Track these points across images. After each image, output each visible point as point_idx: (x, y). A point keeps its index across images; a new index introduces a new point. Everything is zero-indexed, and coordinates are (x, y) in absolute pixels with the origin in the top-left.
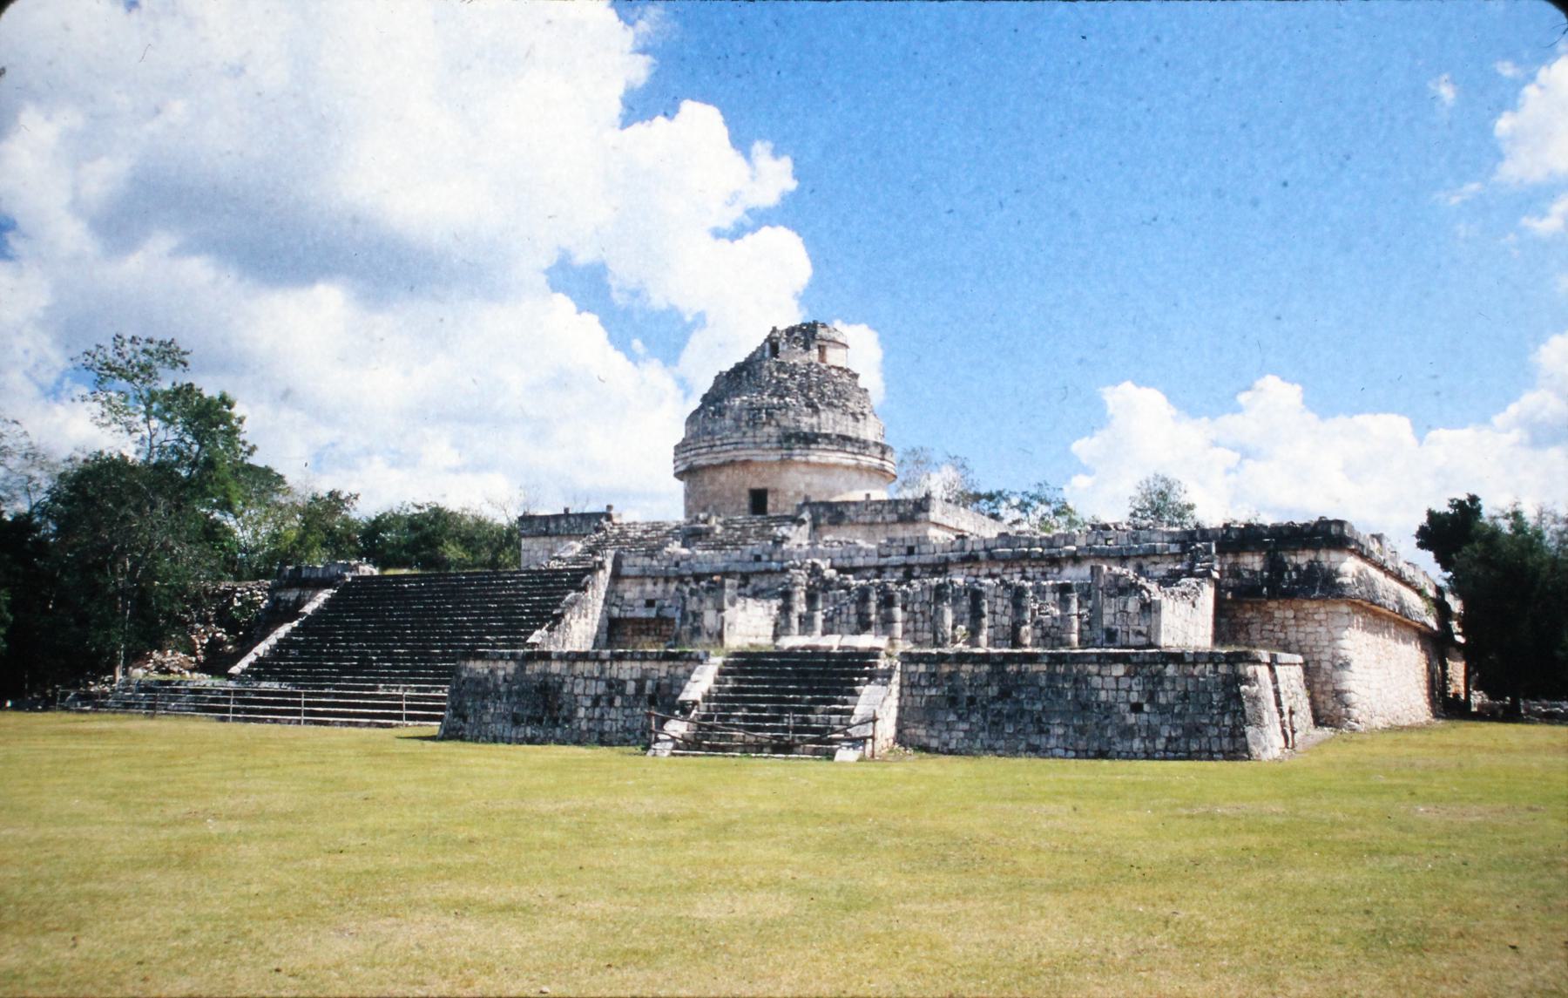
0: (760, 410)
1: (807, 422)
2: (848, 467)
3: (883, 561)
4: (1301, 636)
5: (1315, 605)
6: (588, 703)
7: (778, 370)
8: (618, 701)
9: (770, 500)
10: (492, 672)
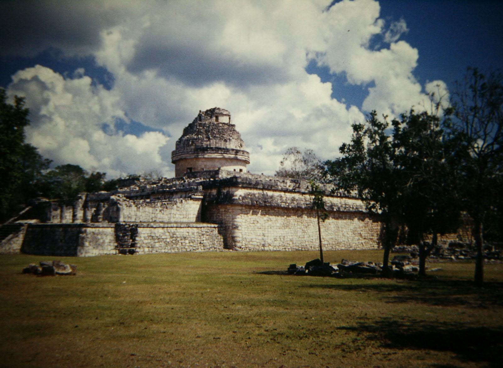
0: (190, 140)
1: (205, 144)
2: (221, 159)
4: (225, 218)
5: (229, 207)
7: (199, 126)
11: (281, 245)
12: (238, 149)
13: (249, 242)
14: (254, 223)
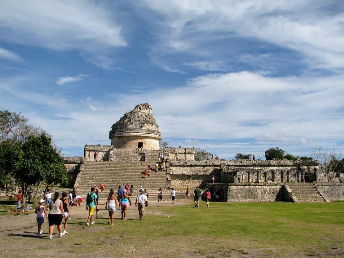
3: (236, 164)
6: (260, 194)
8: (266, 193)
9: (144, 145)
10: (237, 188)
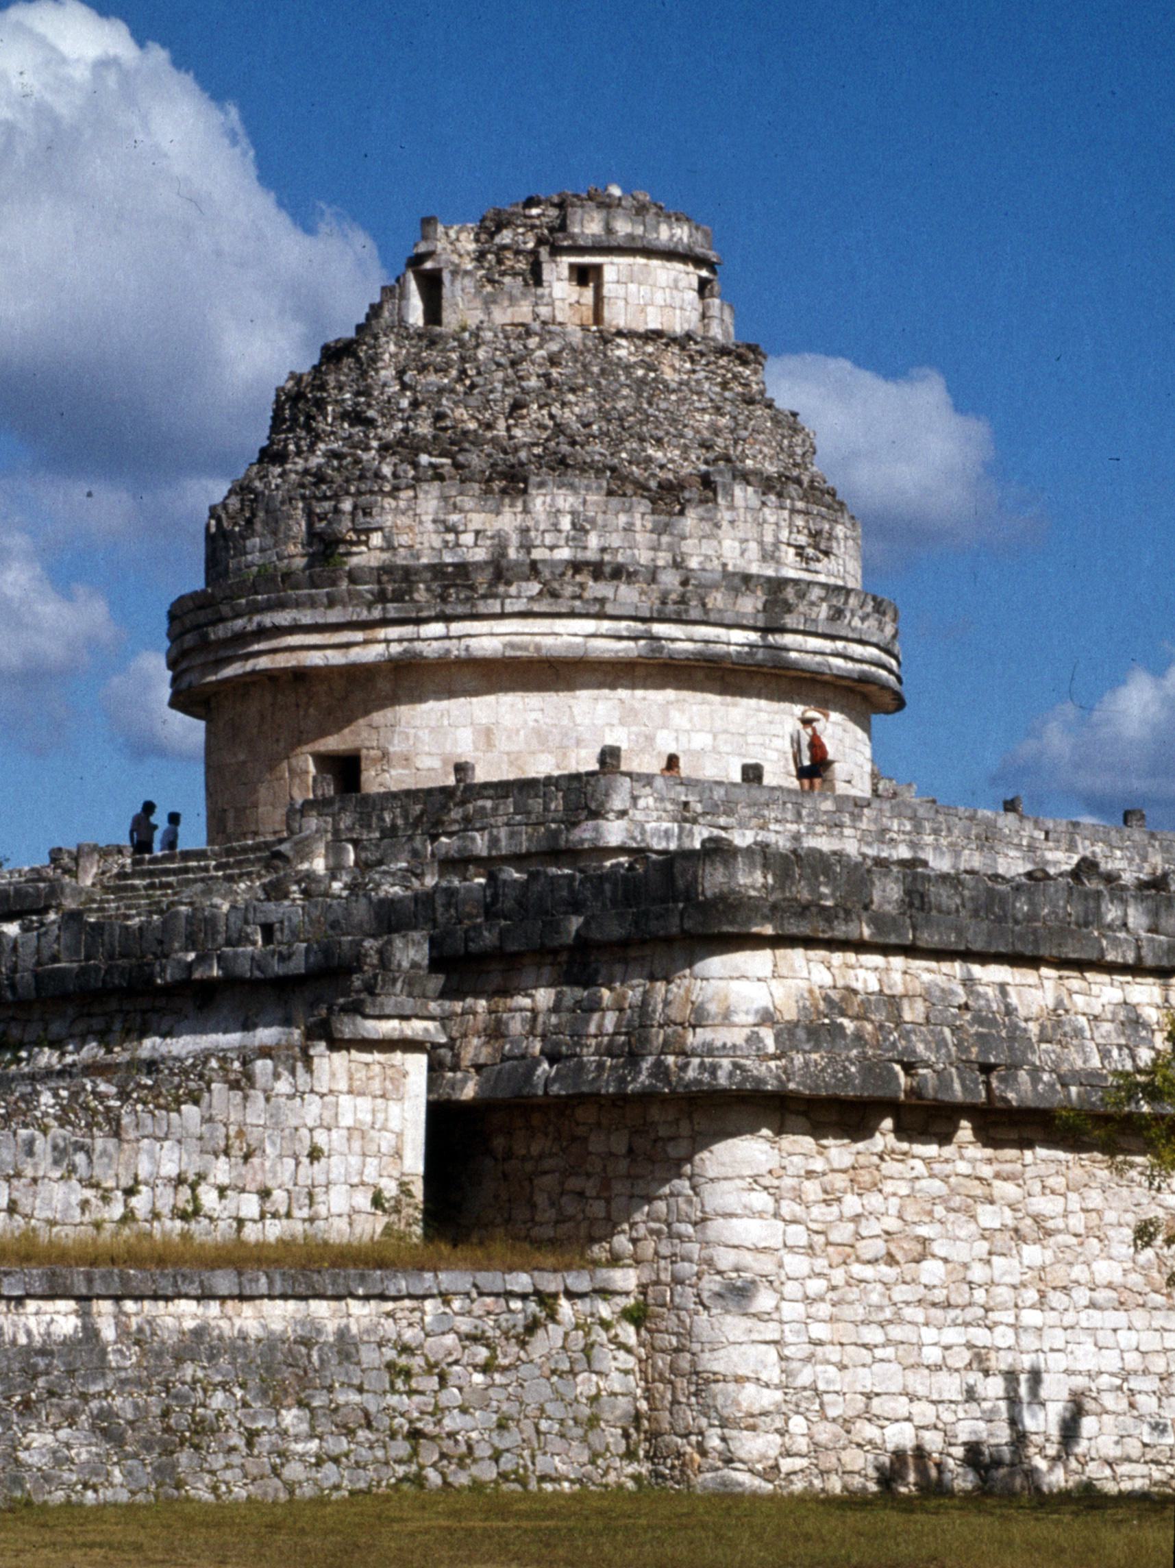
11: (1134, 1449)
12: (791, 570)
13: (846, 1423)
14: (891, 1260)
